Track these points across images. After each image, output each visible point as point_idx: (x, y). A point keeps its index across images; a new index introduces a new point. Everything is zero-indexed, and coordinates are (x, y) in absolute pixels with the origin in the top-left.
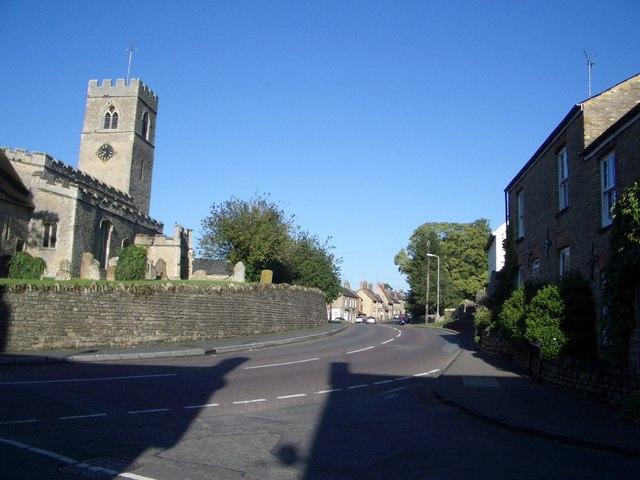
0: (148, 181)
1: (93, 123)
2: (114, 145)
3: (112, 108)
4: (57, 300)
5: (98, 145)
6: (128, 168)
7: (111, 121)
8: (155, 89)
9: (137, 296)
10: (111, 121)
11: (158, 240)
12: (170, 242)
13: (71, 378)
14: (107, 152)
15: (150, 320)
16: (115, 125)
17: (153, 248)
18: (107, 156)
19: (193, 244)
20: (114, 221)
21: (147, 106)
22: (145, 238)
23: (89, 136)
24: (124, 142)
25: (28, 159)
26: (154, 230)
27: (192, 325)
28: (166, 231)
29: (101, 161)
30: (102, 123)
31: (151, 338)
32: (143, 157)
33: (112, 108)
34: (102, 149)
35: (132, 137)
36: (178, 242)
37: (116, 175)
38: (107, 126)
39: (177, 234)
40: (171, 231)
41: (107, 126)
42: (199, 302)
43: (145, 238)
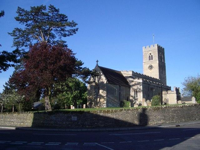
0: (165, 74)
1: (146, 59)
2: (152, 65)
3: (150, 54)
4: (131, 113)
5: (148, 66)
6: (158, 71)
7: (151, 58)
8: (162, 46)
9: (155, 110)
10: (151, 58)
11: (169, 92)
12: (173, 92)
13: (125, 133)
14: (151, 67)
15: (159, 117)
16: (152, 59)
17: (168, 95)
18: (151, 68)
19: (180, 91)
20: (154, 88)
21: (161, 51)
22: (165, 91)
23: (145, 63)
24: (155, 63)
25: (127, 73)
26: (168, 89)
27: (173, 118)
28: (172, 89)
29: (149, 70)
30: (148, 59)
31: (160, 122)
32: (162, 67)
33: (150, 54)
34: (149, 67)
35: (158, 62)
36: (175, 92)
37: (155, 74)
38: (150, 60)
39: (175, 89)
40: (173, 89)
41: (150, 60)
42: (175, 111)
43: (165, 92)
